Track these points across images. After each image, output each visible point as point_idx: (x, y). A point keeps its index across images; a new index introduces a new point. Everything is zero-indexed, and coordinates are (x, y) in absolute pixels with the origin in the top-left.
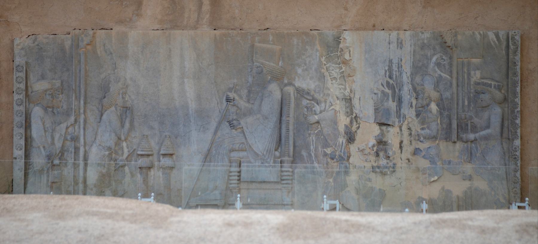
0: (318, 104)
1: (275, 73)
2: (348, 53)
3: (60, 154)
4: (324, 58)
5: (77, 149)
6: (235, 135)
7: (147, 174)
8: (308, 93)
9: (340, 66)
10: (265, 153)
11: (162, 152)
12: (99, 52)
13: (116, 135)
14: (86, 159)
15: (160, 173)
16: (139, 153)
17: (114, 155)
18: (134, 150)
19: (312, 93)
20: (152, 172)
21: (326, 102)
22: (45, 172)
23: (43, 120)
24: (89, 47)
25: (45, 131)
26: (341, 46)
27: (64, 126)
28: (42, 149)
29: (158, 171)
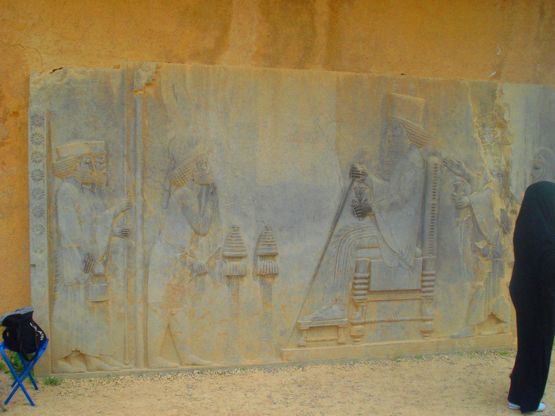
0: (469, 181)
1: (419, 137)
2: (507, 111)
3: (105, 258)
4: (476, 118)
5: (130, 249)
6: (363, 226)
7: (238, 284)
8: (459, 167)
9: (496, 129)
10: (404, 251)
11: (260, 252)
12: (164, 98)
13: (193, 228)
14: (146, 266)
15: (257, 284)
16: (227, 253)
17: (190, 258)
18: (220, 249)
19: (463, 165)
20: (246, 282)
21: (479, 179)
22: (82, 286)
23: (77, 204)
24: (150, 90)
25: (80, 222)
26: (498, 101)
27: (110, 212)
28: (76, 251)
29: (254, 280)
